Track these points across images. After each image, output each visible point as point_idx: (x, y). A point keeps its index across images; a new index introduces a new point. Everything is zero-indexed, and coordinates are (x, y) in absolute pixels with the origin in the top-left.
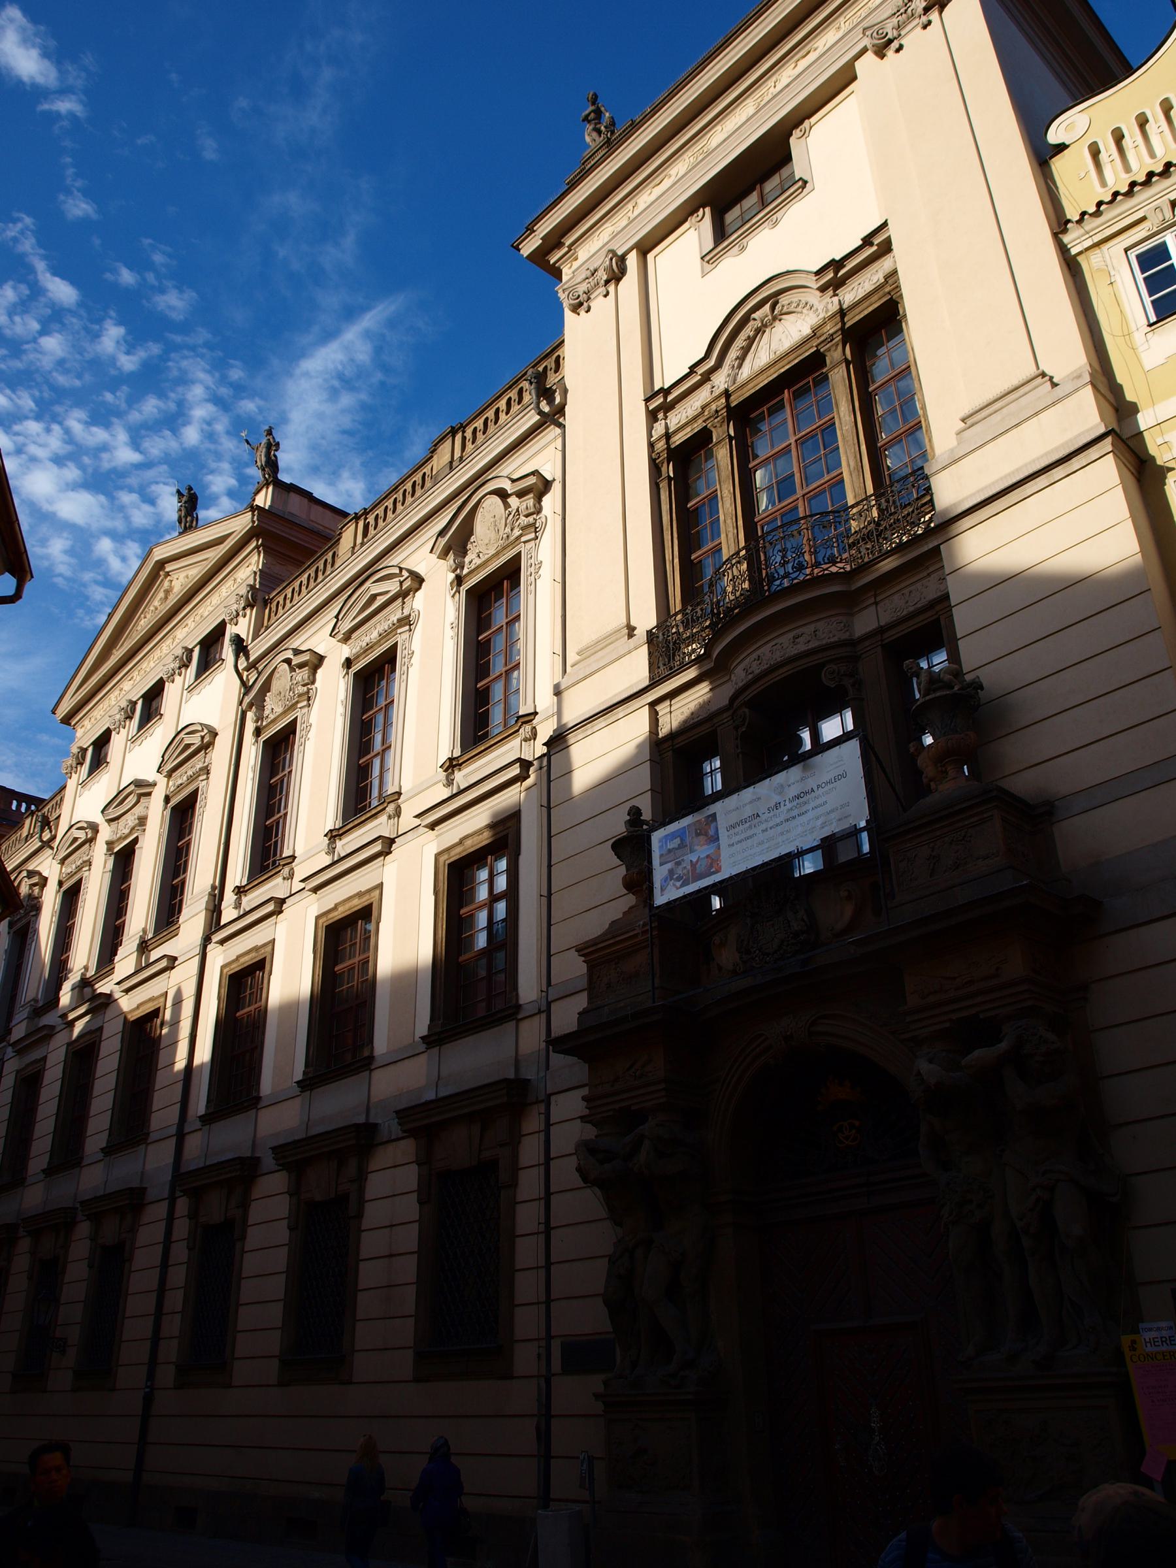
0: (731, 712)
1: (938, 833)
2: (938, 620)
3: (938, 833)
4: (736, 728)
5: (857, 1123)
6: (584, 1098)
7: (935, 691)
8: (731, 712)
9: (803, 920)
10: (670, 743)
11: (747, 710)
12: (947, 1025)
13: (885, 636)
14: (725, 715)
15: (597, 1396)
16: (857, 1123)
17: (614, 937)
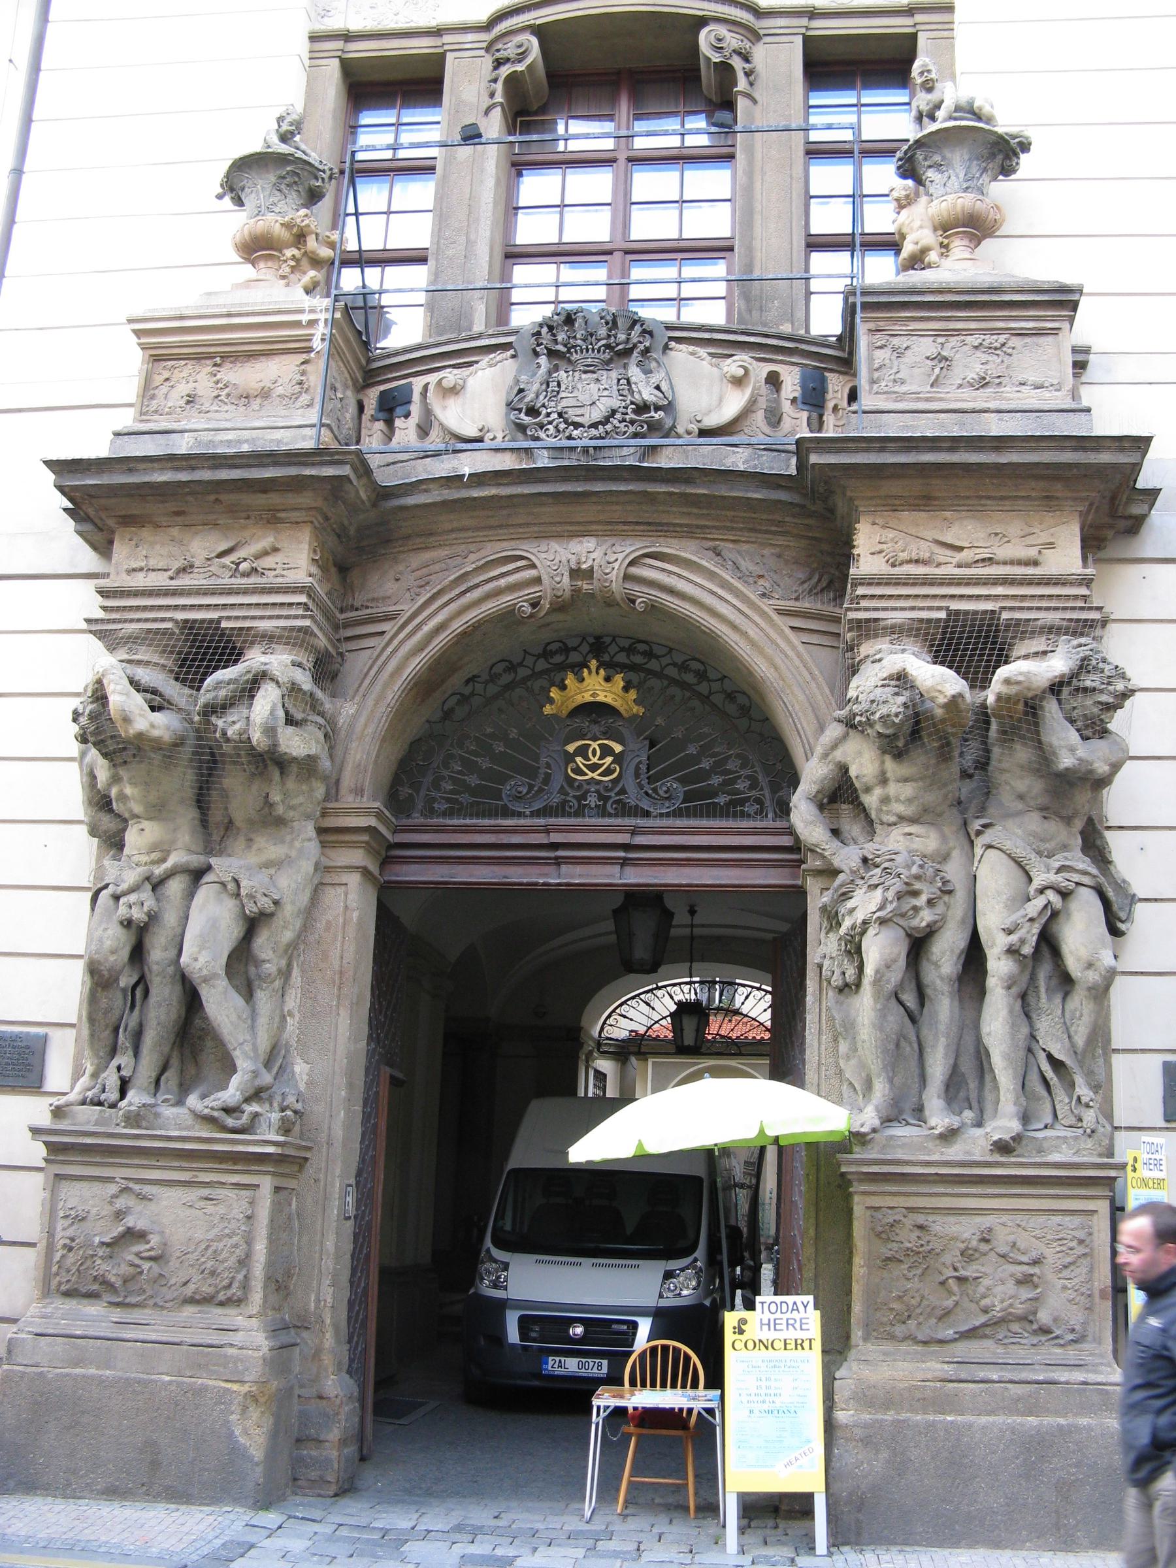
0: (487, 37)
1: (960, 325)
2: (913, 37)
3: (960, 325)
4: (498, 63)
5: (618, 748)
6: (103, 593)
7: (955, 119)
8: (487, 37)
9: (658, 388)
10: (339, 44)
11: (535, 41)
12: (942, 615)
13: (817, 23)
14: (470, 37)
15: (36, 1131)
16: (618, 748)
17: (229, 315)
